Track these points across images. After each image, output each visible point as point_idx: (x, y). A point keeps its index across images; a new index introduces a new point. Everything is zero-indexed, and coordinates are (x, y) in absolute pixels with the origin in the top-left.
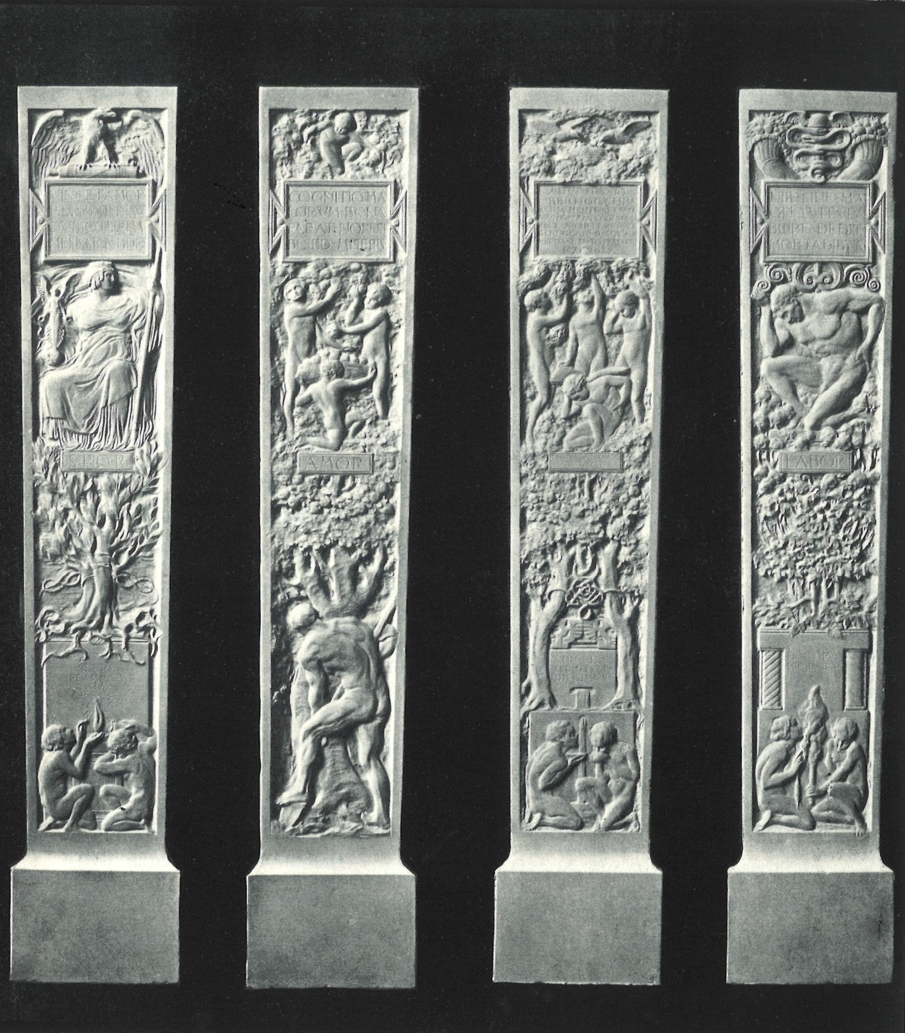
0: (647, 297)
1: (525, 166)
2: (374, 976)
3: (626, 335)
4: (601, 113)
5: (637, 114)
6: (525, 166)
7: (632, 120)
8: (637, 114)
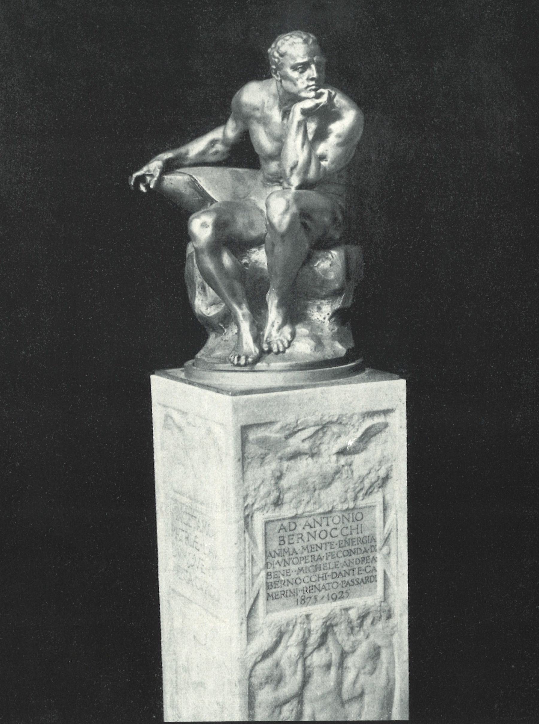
0: (391, 645)
1: (249, 501)
2: (347, 718)
3: (367, 699)
4: (335, 419)
5: (371, 414)
6: (249, 501)
7: (369, 423)
8: (371, 414)
